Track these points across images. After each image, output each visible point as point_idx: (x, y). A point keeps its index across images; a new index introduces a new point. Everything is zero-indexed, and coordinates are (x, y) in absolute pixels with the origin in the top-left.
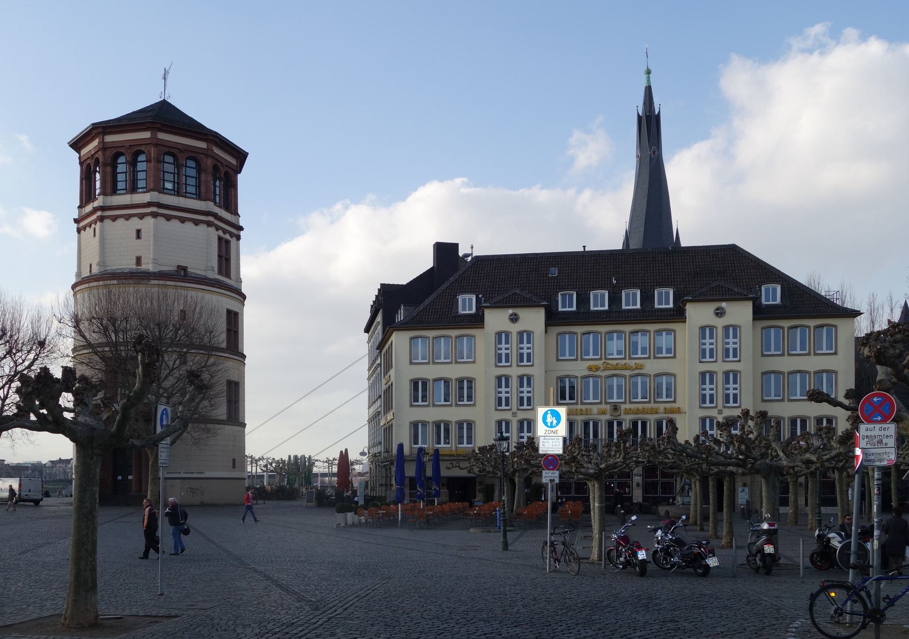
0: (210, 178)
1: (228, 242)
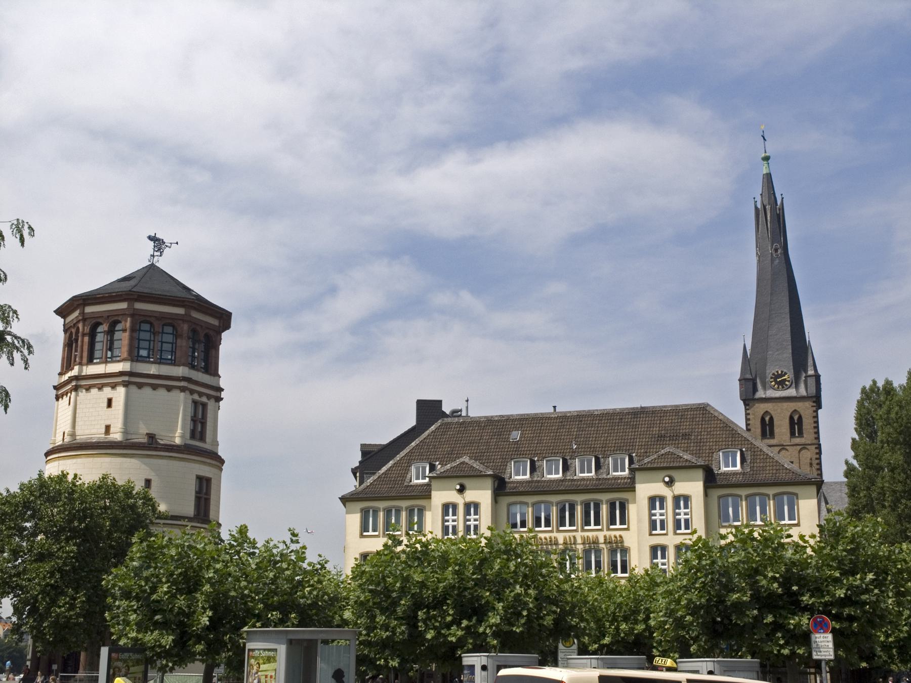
1: (204, 405)
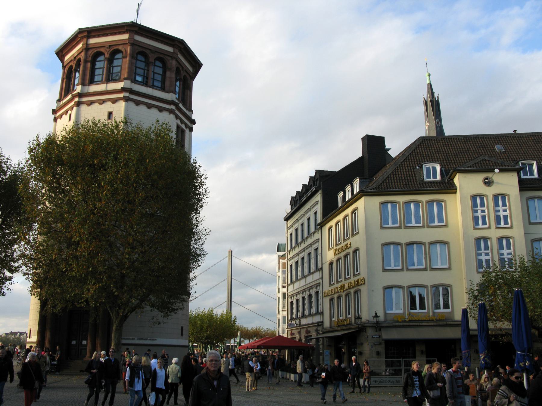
0: (173, 76)
1: (183, 131)
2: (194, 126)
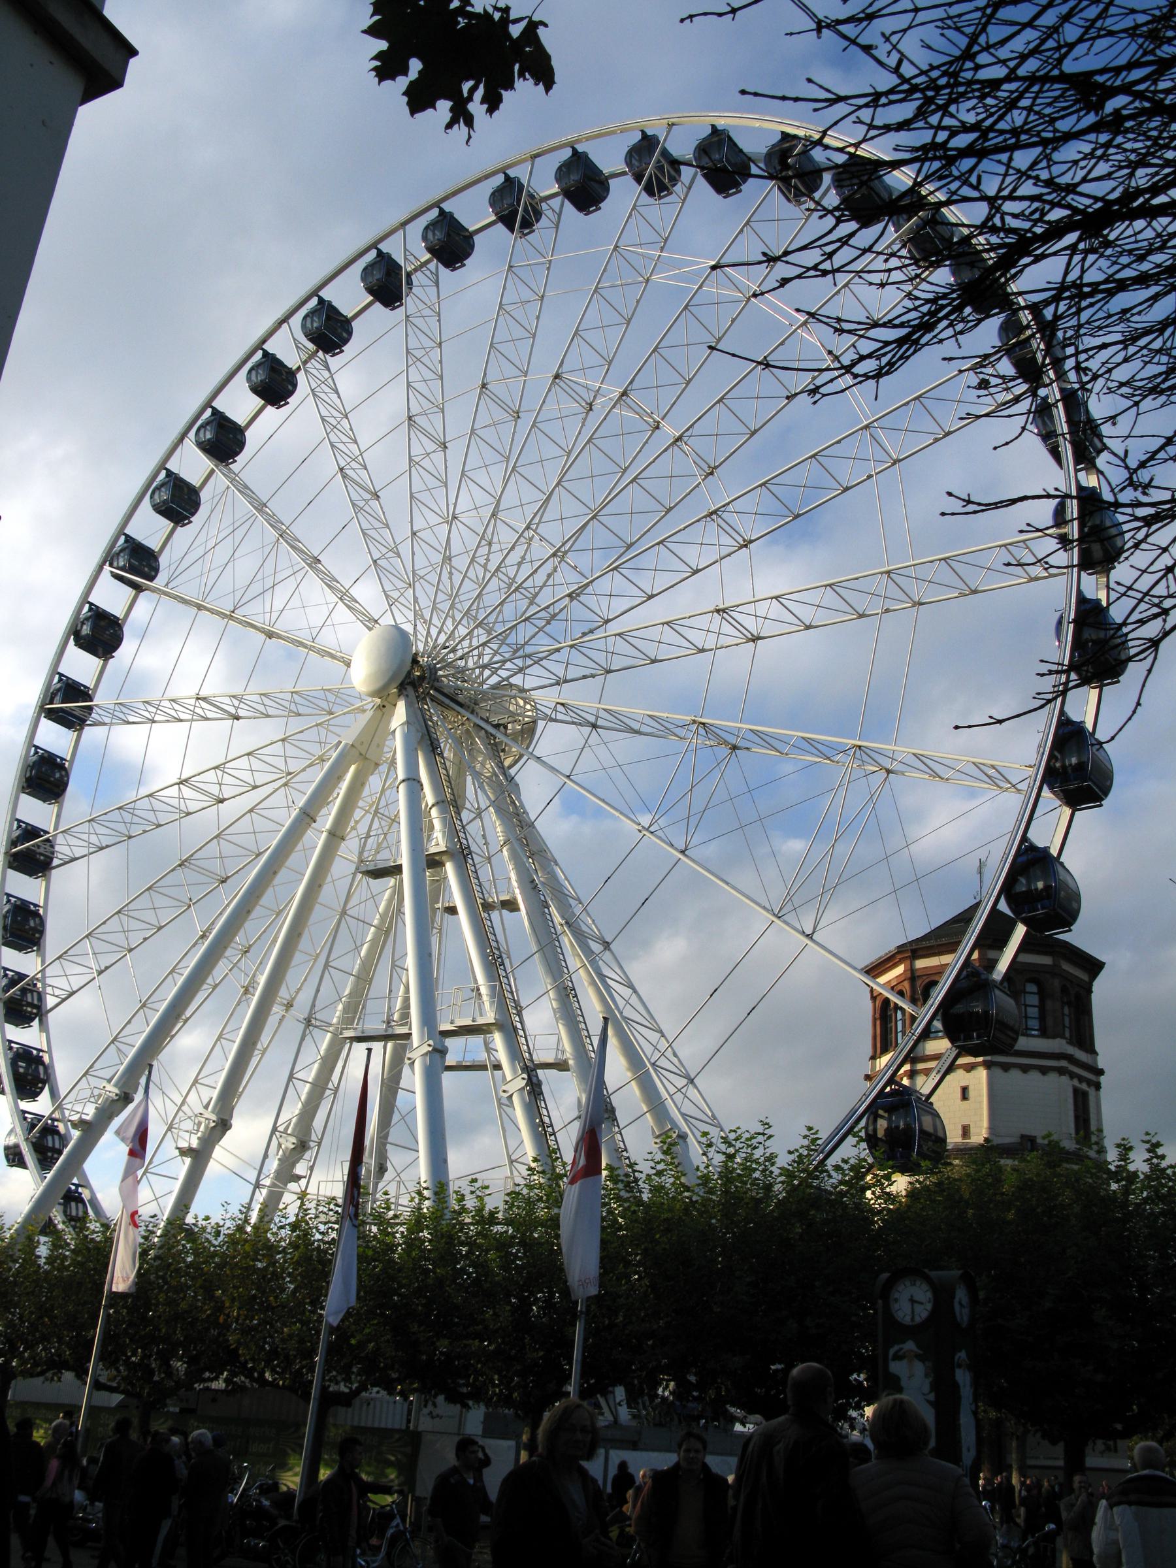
1: (1085, 1095)
2: (1102, 1079)
